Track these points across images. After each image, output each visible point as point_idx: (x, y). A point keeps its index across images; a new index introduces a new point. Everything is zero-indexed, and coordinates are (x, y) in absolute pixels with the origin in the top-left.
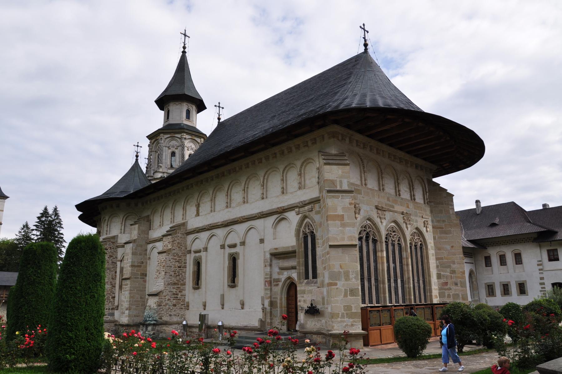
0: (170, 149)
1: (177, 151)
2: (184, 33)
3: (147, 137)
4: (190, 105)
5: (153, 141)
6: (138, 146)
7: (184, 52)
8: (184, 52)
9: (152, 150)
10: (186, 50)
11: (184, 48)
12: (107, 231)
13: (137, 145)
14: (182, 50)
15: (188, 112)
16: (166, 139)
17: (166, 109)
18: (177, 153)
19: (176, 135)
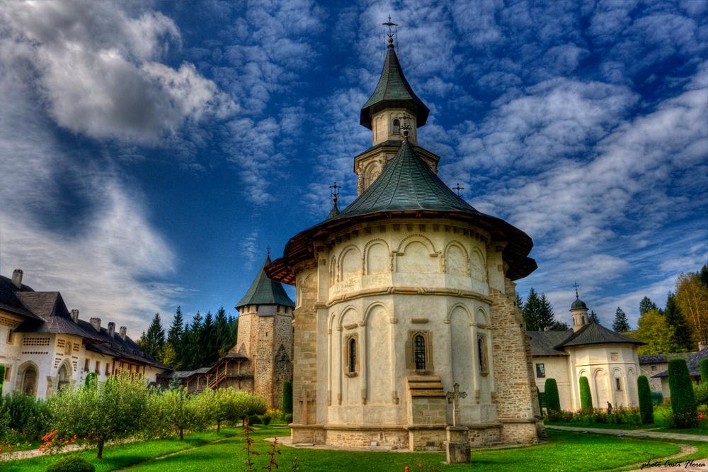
2: (387, 21)
6: (335, 187)
13: (333, 185)
15: (396, 122)
16: (366, 168)
19: (375, 159)
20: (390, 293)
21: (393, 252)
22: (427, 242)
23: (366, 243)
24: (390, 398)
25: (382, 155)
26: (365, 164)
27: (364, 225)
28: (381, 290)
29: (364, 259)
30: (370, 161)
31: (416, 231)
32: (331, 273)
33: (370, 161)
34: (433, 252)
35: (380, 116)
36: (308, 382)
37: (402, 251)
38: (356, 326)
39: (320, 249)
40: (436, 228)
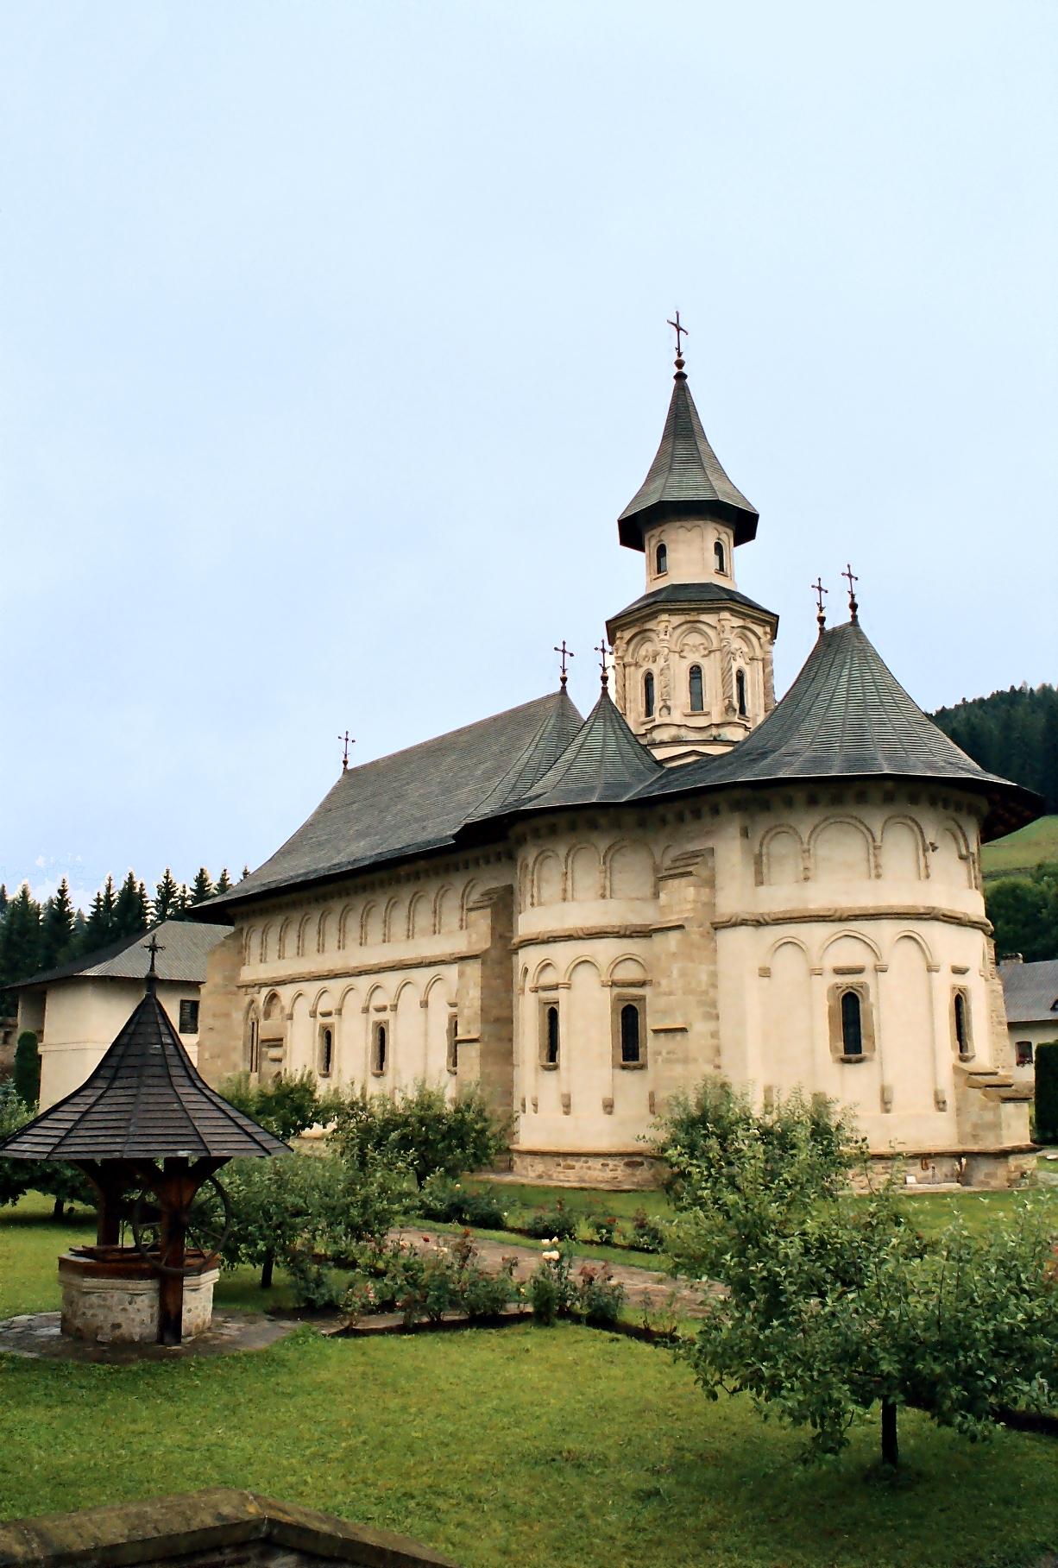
0: (684, 657)
1: (704, 663)
3: (608, 623)
4: (721, 528)
5: (627, 635)
7: (680, 377)
8: (680, 377)
9: (626, 660)
10: (684, 370)
11: (680, 364)
12: (565, 890)
14: (676, 370)
15: (719, 548)
17: (652, 545)
18: (705, 666)
19: (704, 618)
20: (936, 919)
21: (932, 844)
22: (960, 835)
23: (886, 817)
24: (931, 1101)
25: (726, 615)
26: (677, 620)
27: (889, 785)
28: (922, 911)
29: (880, 847)
30: (689, 618)
31: (951, 812)
32: (761, 855)
33: (689, 618)
34: (964, 852)
35: (688, 524)
36: (709, 1069)
37: (936, 845)
38: (860, 971)
39: (738, 806)
40: (972, 811)
